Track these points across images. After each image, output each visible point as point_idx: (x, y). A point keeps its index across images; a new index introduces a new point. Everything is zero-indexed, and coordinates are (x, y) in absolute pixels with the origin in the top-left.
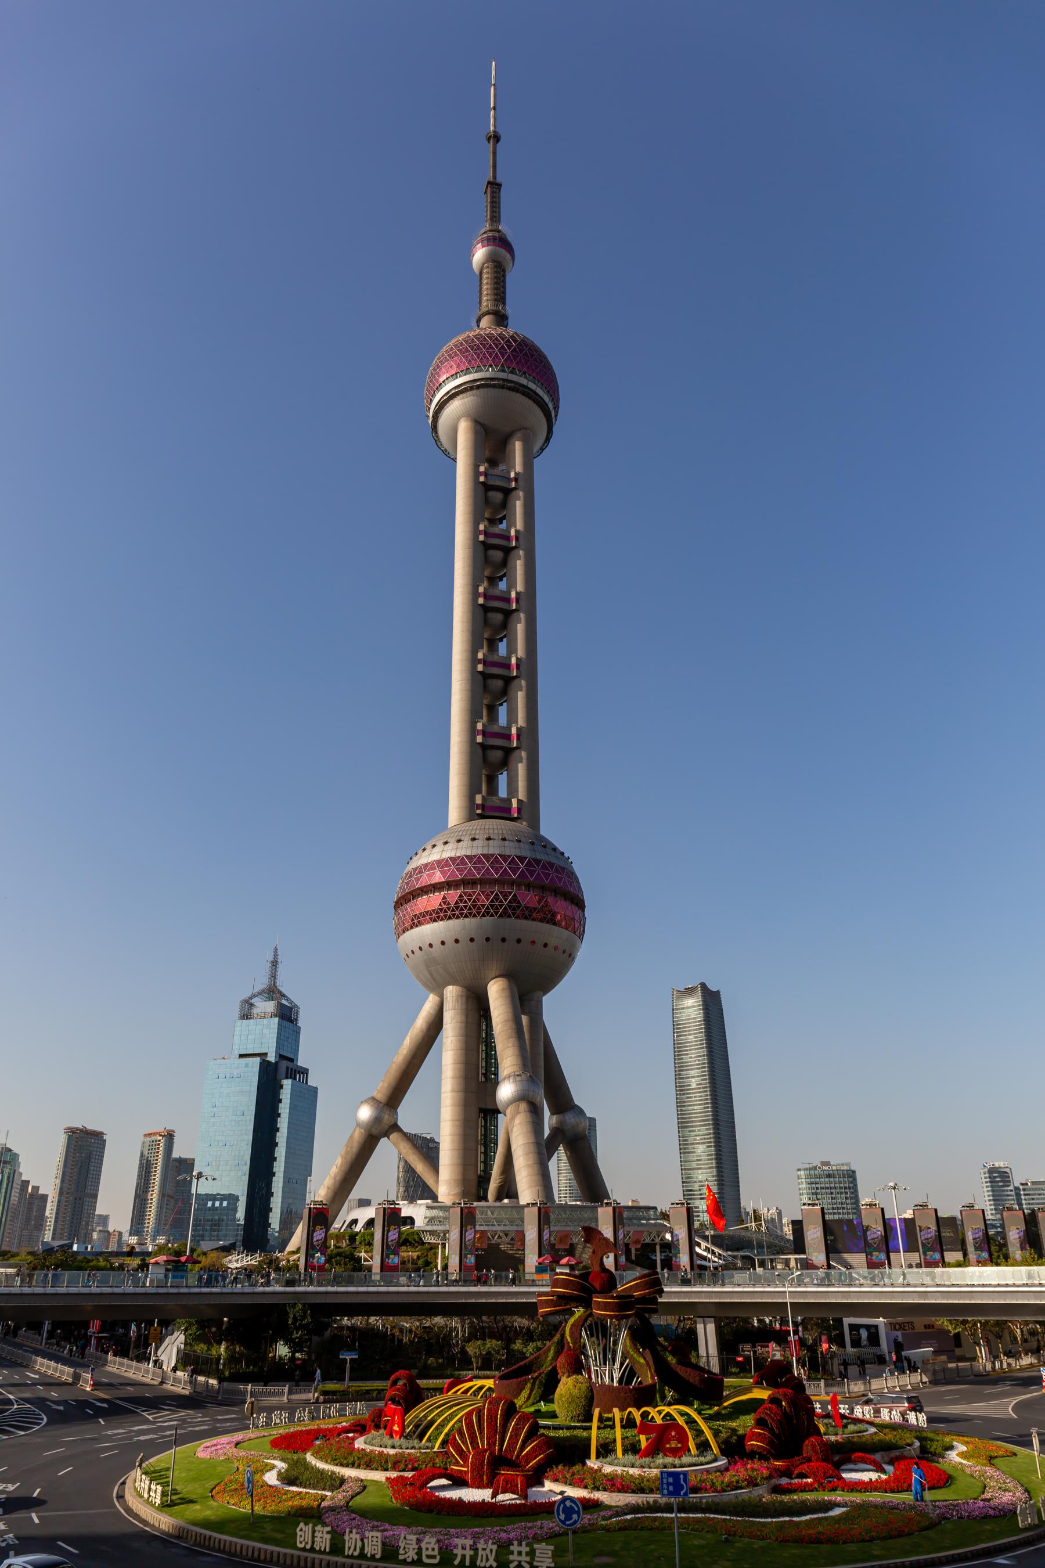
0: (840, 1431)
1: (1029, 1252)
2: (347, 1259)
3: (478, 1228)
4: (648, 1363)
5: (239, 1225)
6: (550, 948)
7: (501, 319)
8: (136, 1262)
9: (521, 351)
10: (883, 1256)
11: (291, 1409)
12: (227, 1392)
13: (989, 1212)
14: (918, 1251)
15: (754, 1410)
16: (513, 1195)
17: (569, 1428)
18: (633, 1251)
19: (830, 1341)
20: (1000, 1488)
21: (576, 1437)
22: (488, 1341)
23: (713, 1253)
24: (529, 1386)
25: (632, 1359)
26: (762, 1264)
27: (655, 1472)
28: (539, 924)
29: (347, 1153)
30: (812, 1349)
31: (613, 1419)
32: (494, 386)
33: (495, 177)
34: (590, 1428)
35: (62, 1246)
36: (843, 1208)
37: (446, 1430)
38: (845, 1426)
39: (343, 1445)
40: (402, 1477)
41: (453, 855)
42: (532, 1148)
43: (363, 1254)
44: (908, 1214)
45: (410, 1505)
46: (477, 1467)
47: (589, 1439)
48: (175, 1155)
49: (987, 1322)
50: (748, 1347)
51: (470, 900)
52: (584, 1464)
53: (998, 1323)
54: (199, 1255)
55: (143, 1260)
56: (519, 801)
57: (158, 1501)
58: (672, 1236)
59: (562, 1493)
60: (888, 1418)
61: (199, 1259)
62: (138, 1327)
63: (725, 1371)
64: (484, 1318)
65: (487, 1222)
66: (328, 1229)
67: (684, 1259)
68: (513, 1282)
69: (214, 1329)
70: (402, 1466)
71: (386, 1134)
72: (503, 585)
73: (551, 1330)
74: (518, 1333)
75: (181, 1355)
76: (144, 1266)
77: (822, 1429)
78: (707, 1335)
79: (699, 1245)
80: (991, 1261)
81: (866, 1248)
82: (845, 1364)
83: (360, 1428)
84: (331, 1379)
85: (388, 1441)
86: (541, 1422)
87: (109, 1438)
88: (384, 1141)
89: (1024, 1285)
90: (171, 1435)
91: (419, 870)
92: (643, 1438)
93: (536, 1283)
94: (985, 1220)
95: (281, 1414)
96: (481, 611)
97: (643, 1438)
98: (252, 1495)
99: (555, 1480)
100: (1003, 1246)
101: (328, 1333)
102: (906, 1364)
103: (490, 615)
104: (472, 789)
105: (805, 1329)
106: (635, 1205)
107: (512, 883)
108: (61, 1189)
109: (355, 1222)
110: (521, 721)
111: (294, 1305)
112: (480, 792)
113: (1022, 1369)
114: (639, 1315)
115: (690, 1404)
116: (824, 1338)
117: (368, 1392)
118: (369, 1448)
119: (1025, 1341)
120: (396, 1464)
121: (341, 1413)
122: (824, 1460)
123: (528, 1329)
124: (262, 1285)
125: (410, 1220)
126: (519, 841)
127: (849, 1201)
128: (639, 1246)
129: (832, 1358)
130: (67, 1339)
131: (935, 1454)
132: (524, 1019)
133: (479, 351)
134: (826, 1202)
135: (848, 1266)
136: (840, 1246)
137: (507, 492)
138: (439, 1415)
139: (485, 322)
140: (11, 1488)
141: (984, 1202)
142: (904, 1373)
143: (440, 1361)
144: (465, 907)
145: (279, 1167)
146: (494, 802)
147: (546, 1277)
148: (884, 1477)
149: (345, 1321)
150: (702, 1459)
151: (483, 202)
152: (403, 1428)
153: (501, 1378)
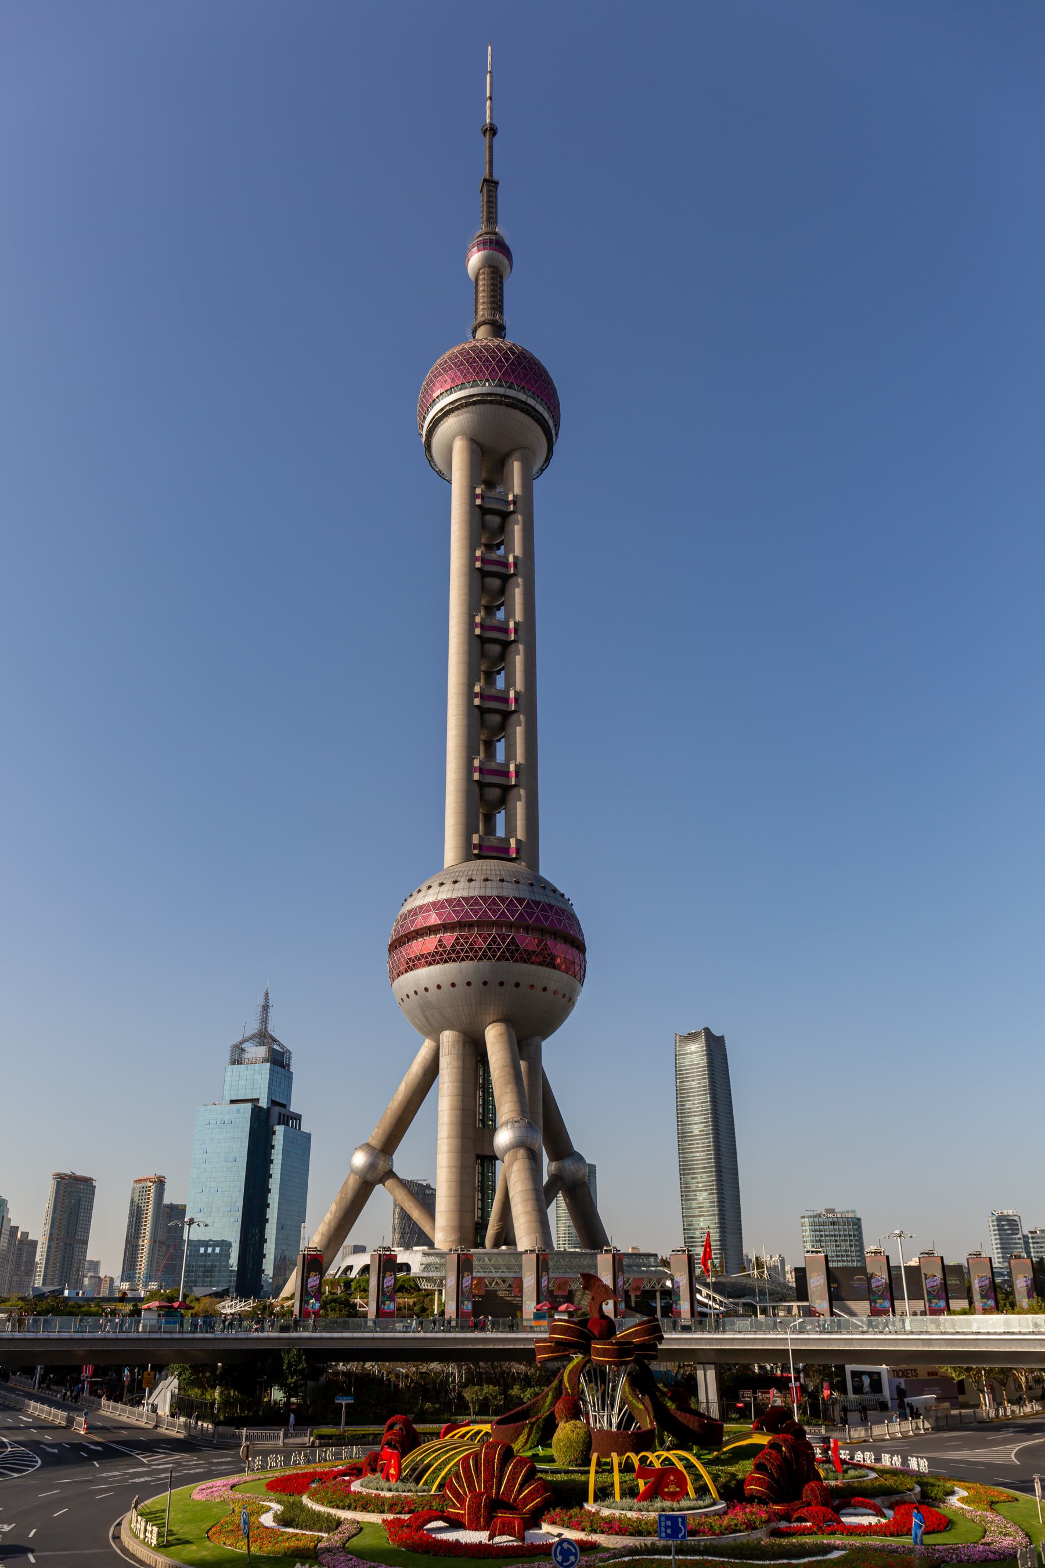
0: (840, 1476)
1: (1036, 1300)
2: (342, 1305)
3: (475, 1275)
4: (646, 1409)
5: (232, 1271)
6: (549, 992)
7: (498, 329)
8: (128, 1308)
9: (520, 364)
10: (887, 1304)
11: (286, 1453)
12: (222, 1435)
13: (997, 1260)
14: (923, 1299)
15: (754, 1455)
16: (511, 1241)
17: (566, 1472)
18: (633, 1298)
19: (832, 1388)
20: (1000, 1533)
21: (573, 1481)
22: (485, 1386)
23: (714, 1300)
24: (526, 1430)
25: (631, 1404)
26: (764, 1311)
27: (653, 1515)
28: (539, 967)
29: (341, 1198)
30: (814, 1396)
31: (611, 1464)
32: (491, 402)
33: (491, 174)
34: (588, 1472)
35: (53, 1291)
36: (848, 1256)
37: (443, 1474)
38: (846, 1472)
39: (339, 1487)
40: (399, 1519)
41: (449, 896)
42: (531, 1195)
43: (358, 1301)
44: (914, 1262)
45: (406, 1546)
46: (475, 1509)
47: (587, 1483)
48: (166, 1201)
49: (991, 1370)
50: (748, 1393)
51: (466, 943)
52: (582, 1507)
53: (1002, 1371)
54: (192, 1301)
55: (135, 1306)
56: (518, 841)
57: (154, 1542)
58: (673, 1283)
59: (559, 1535)
60: (888, 1464)
61: (192, 1305)
62: (131, 1371)
63: (725, 1417)
64: (481, 1364)
65: (485, 1268)
66: (322, 1275)
67: (684, 1306)
68: (512, 1328)
69: (208, 1374)
70: (399, 1509)
71: (382, 1180)
72: (500, 615)
73: (549, 1376)
74: (515, 1379)
75: (175, 1399)
76: (136, 1313)
77: (822, 1474)
78: (707, 1382)
79: (700, 1292)
80: (998, 1309)
81: (868, 1294)
82: (845, 1410)
83: (356, 1472)
84: (327, 1424)
85: (383, 1483)
86: (539, 1466)
87: (104, 1481)
88: (379, 1187)
89: (1030, 1333)
90: (167, 1478)
91: (415, 912)
92: (641, 1482)
93: (534, 1330)
94: (992, 1268)
95: (277, 1458)
97: (641, 1482)
98: (248, 1537)
99: (553, 1523)
100: (1010, 1294)
101: (323, 1379)
102: (908, 1411)
103: (487, 646)
104: (469, 828)
105: (807, 1375)
106: (636, 1252)
107: (510, 925)
108: (51, 1235)
109: (350, 1268)
110: (520, 758)
111: (289, 1351)
112: (477, 832)
113: (1026, 1416)
114: (636, 1361)
115: (689, 1449)
116: (825, 1384)
117: (364, 1436)
118: (365, 1491)
119: (1030, 1388)
120: (393, 1506)
121: (337, 1456)
122: (823, 1505)
123: (526, 1375)
124: (256, 1330)
125: (407, 1267)
126: (517, 882)
127: (853, 1249)
128: (639, 1293)
129: (833, 1404)
130: (60, 1382)
131: (935, 1499)
132: (523, 1065)
133: (475, 364)
134: (830, 1249)
135: (852, 1314)
136: (844, 1294)
137: (505, 516)
138: (435, 1459)
139: (481, 333)
140: (6, 1528)
141: (992, 1250)
142: (906, 1419)
143: (437, 1406)
144: (462, 950)
145: (272, 1214)
146: (492, 841)
147: (545, 1323)
148: (883, 1521)
149: (341, 1366)
150: (701, 1503)
151: (479, 201)
152: (399, 1471)
153: (499, 1423)
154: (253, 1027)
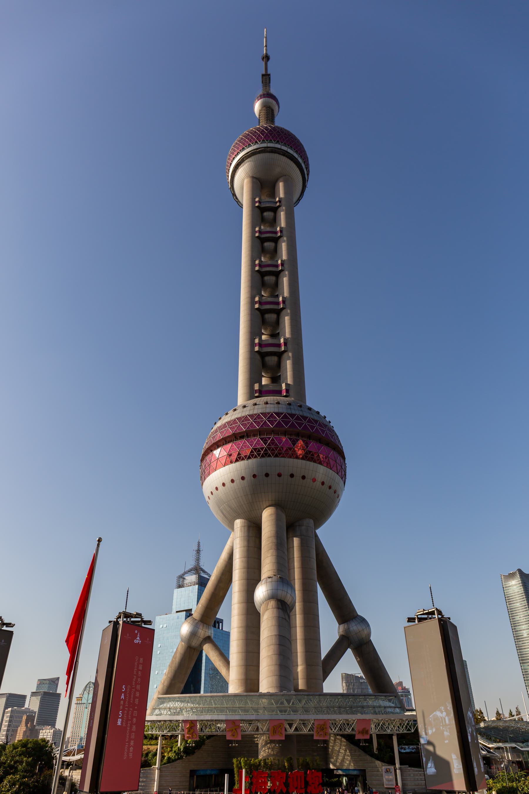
96: (258, 276)
154: (191, 564)
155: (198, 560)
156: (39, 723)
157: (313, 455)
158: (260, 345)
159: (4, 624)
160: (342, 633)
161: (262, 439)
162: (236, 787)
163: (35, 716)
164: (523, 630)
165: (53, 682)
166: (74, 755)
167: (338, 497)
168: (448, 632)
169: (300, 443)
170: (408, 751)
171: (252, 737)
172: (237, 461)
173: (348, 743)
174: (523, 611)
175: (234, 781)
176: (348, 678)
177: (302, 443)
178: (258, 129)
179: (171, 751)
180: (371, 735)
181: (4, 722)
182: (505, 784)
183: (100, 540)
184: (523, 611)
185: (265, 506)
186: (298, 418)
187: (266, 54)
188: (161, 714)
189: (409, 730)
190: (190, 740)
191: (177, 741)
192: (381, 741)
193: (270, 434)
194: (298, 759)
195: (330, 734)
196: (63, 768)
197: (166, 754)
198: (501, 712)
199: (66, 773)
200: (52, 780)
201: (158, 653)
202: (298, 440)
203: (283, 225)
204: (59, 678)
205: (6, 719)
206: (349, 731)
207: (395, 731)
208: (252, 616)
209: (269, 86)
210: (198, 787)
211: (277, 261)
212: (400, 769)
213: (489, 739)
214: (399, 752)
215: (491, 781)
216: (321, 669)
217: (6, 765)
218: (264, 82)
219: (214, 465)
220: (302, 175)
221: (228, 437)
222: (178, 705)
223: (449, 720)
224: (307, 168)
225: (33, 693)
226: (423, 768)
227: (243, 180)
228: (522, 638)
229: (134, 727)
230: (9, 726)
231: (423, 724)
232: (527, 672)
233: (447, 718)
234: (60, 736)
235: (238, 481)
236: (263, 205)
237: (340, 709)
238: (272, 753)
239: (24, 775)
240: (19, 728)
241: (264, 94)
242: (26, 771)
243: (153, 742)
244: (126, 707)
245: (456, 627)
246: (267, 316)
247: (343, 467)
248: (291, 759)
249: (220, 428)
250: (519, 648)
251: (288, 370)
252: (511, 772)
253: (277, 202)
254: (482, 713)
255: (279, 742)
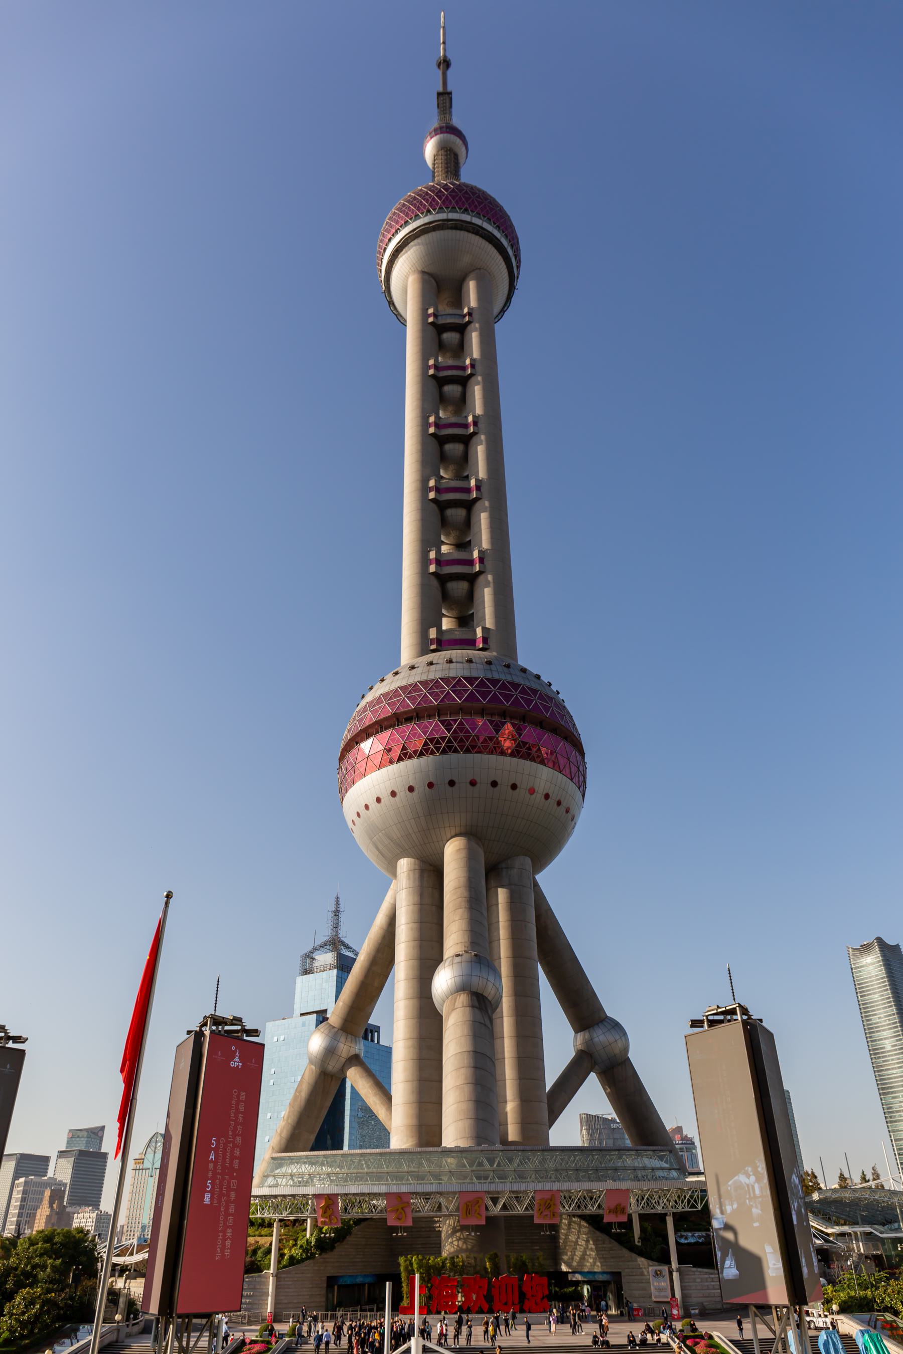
6: (522, 792)
96: (434, 443)
154: (325, 934)
155: (336, 927)
156: (72, 1203)
157: (529, 749)
158: (438, 562)
159: (9, 1038)
160: (580, 1047)
161: (443, 722)
162: (405, 1303)
163: (64, 1191)
164: (885, 1039)
165: (94, 1133)
166: (131, 1254)
167: (572, 819)
168: (758, 1044)
169: (508, 728)
170: (691, 1240)
171: (430, 1220)
172: (400, 759)
173: (592, 1229)
174: (885, 1008)
175: (401, 1292)
176: (591, 1122)
177: (511, 728)
178: (432, 189)
179: (295, 1245)
180: (630, 1216)
181: (13, 1201)
182: (853, 1293)
183: (169, 896)
184: (885, 1008)
185: (449, 836)
186: (504, 686)
187: (445, 56)
188: (276, 1186)
189: (693, 1206)
190: (326, 1227)
191: (305, 1230)
192: (646, 1224)
193: (457, 714)
194: (508, 1257)
195: (561, 1215)
196: (114, 1276)
197: (286, 1251)
198: (846, 1175)
199: (120, 1283)
200: (96, 1295)
201: (272, 1082)
202: (503, 724)
203: (476, 354)
204: (103, 1127)
205: (17, 1196)
206: (592, 1209)
207: (670, 1208)
208: (428, 1020)
209: (450, 113)
210: (340, 1305)
211: (466, 417)
212: (679, 1270)
213: (827, 1219)
214: (678, 1243)
215: (830, 1288)
216: (545, 1107)
217: (18, 1272)
218: (441, 106)
219: (361, 767)
220: (508, 267)
221: (386, 719)
222: (305, 1169)
223: (761, 1189)
224: (516, 256)
225: (61, 1152)
226: (717, 1269)
227: (407, 278)
228: (882, 1053)
229: (232, 1206)
230: (22, 1207)
231: (716, 1196)
232: (891, 1108)
233: (756, 1186)
234: (108, 1222)
235: (402, 793)
236: (441, 321)
237: (579, 1173)
238: (465, 1247)
239: (48, 1288)
240: (39, 1211)
241: (441, 128)
242: (52, 1282)
243: (265, 1231)
244: (219, 1174)
245: (772, 1035)
246: (450, 512)
247: (581, 768)
248: (496, 1255)
249: (370, 704)
250: (878, 1070)
251: (486, 605)
252: (864, 1273)
253: (464, 316)
254: (816, 1177)
255: (477, 1228)
